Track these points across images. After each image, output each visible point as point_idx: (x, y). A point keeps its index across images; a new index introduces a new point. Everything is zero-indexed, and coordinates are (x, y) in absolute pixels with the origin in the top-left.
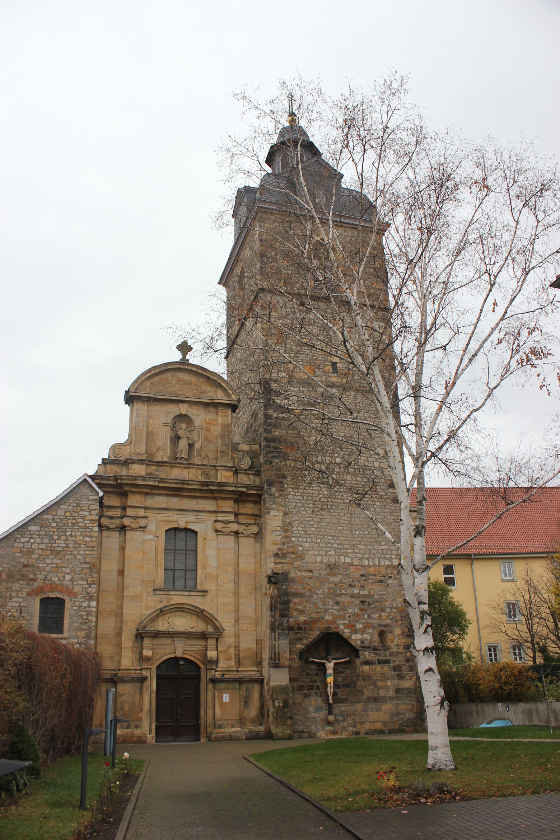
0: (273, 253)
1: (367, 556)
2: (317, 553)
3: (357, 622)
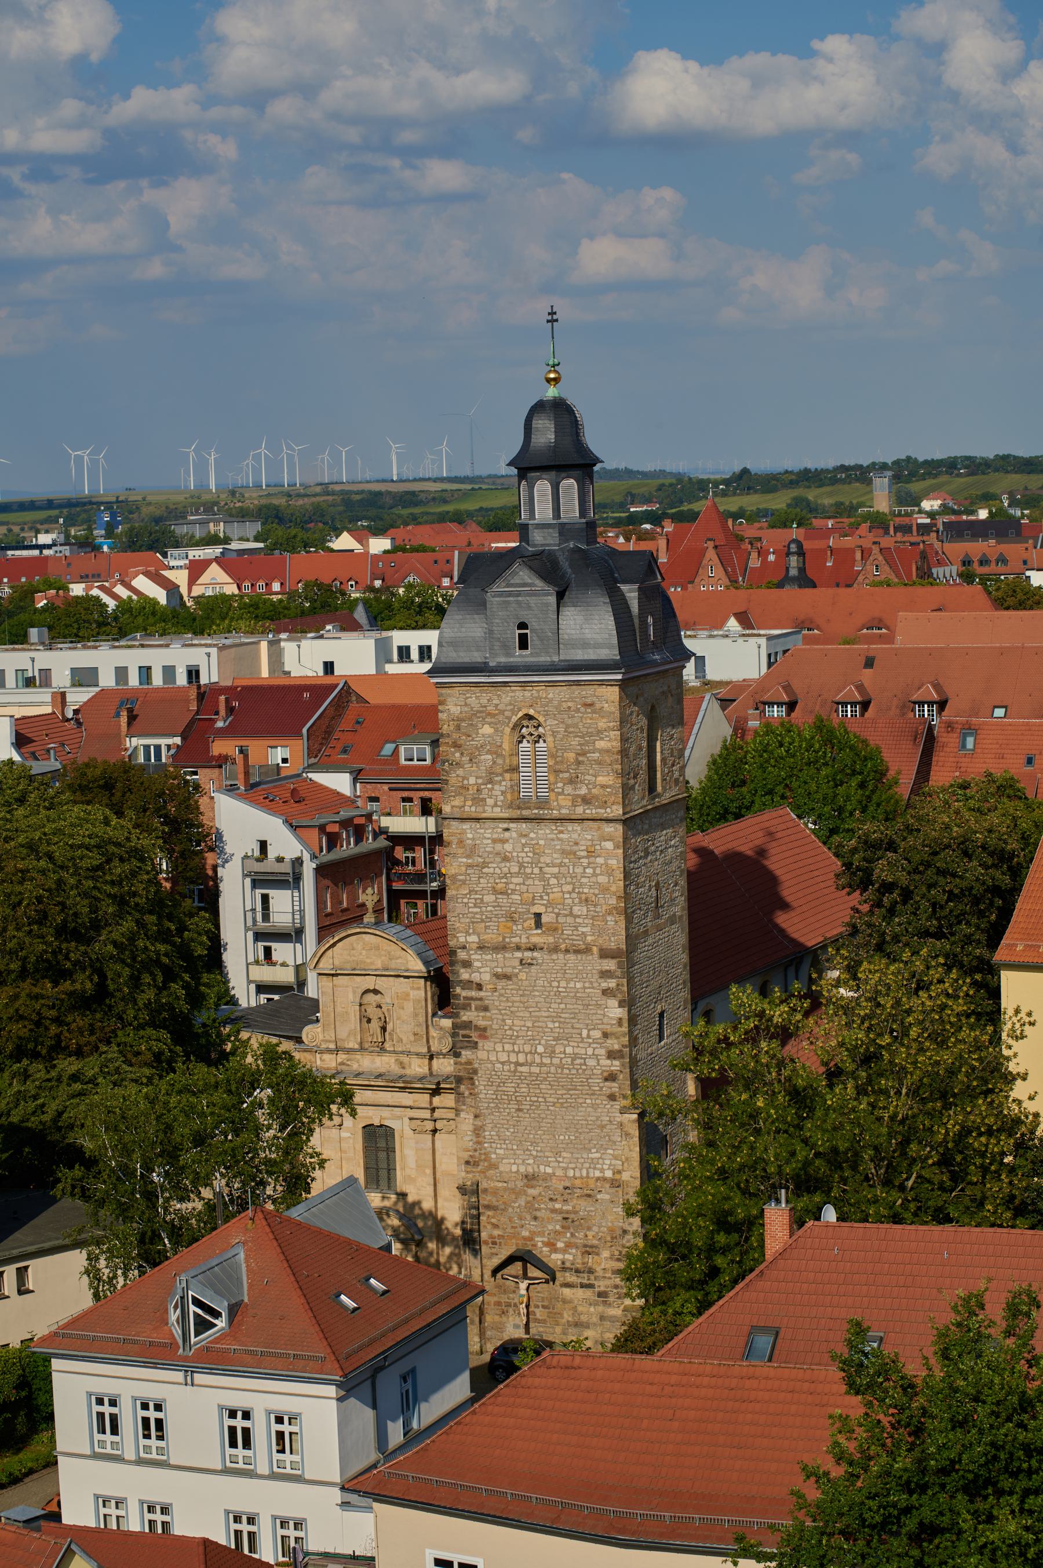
1: (573, 1165)
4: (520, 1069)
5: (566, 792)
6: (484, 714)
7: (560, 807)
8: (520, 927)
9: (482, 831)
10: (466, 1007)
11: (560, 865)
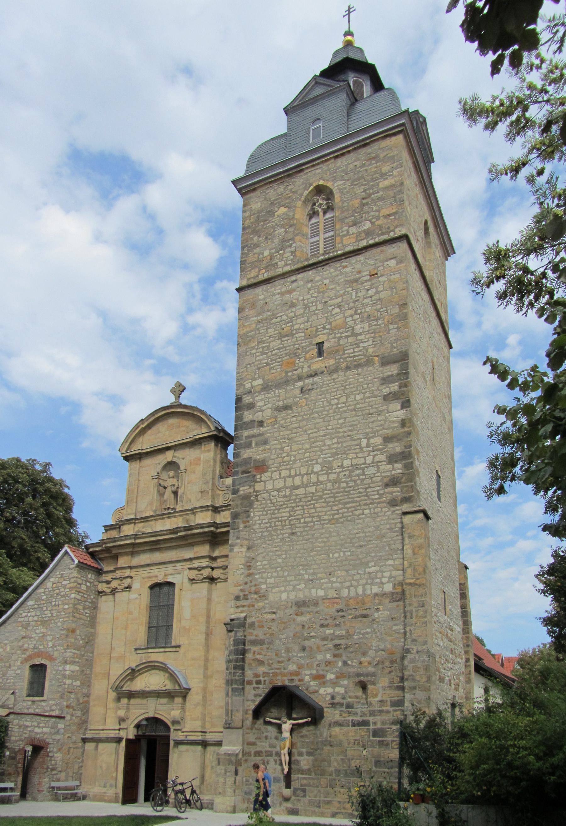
1: (348, 584)
2: (283, 589)
4: (296, 492)
5: (351, 232)
8: (302, 360)
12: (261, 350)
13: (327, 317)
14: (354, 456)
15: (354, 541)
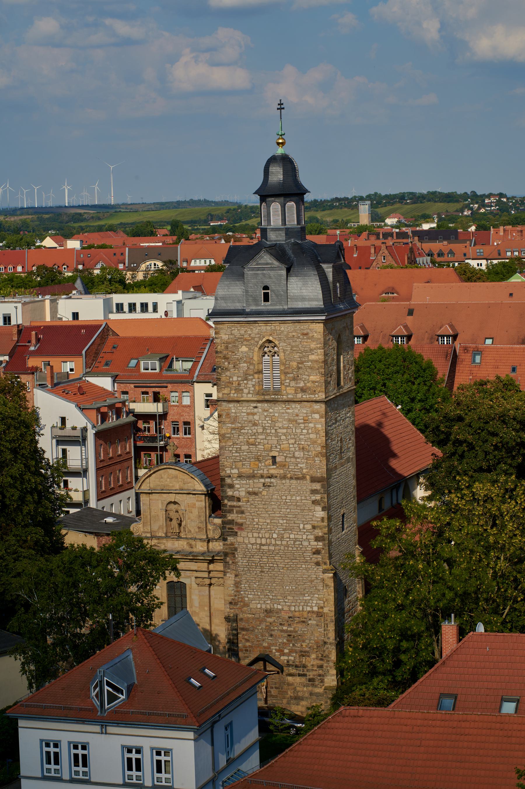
0: (226, 363)
1: (294, 604)
2: (258, 602)
3: (286, 648)
4: (262, 547)
5: (291, 385)
6: (242, 340)
7: (288, 394)
8: (263, 464)
9: (241, 408)
10: (231, 511)
11: (287, 428)
12: (235, 449)
13: (278, 440)
14: (296, 533)
15: (297, 581)
